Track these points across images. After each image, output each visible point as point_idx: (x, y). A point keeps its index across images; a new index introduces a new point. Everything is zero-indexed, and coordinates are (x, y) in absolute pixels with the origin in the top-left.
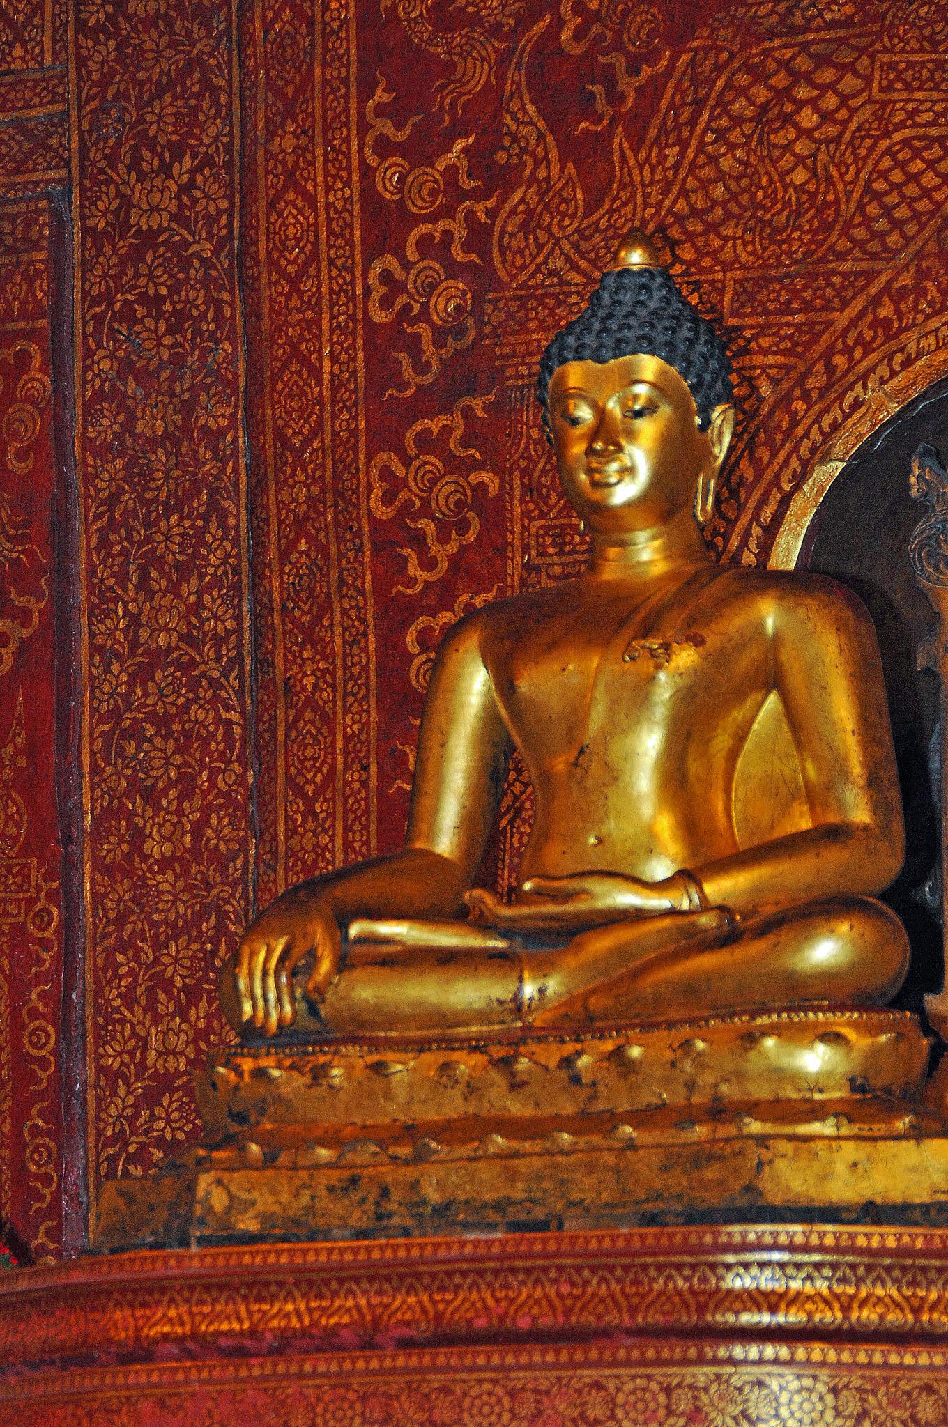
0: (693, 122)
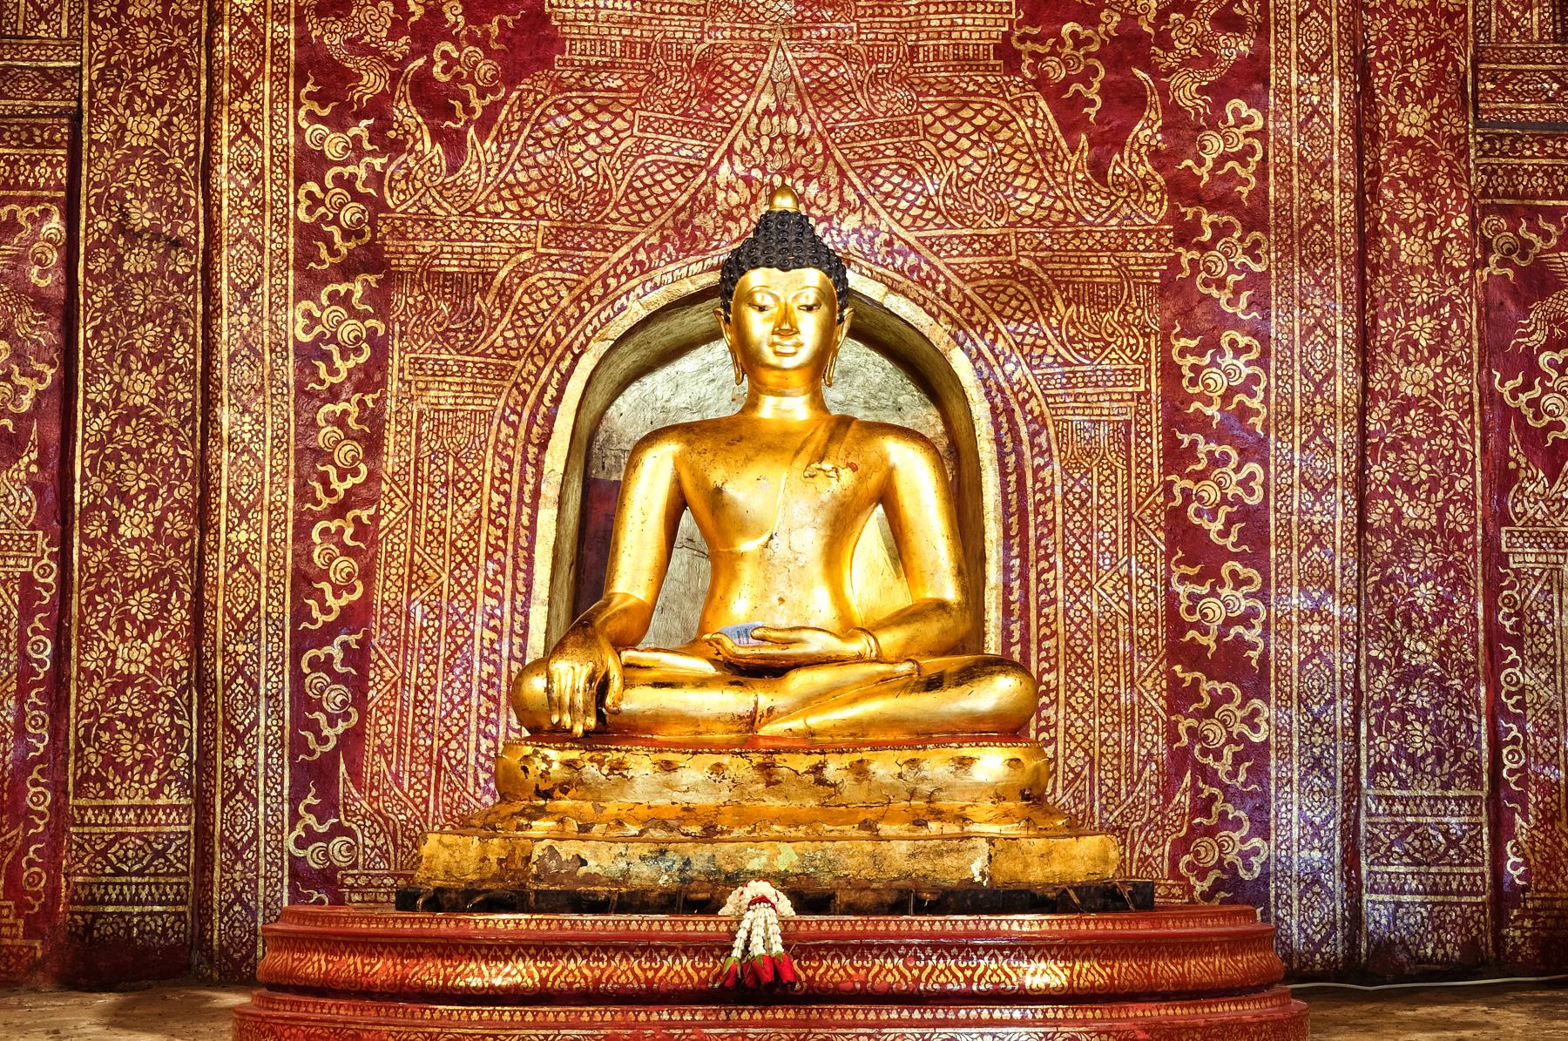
0: (520, 131)
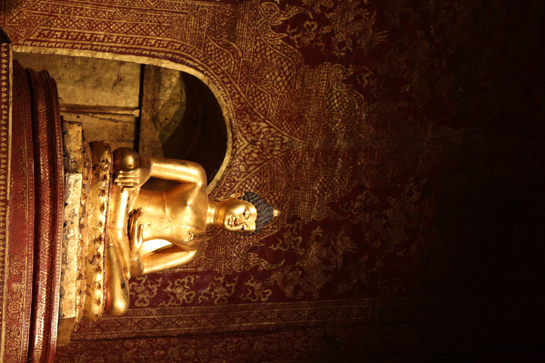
0: (284, 53)
